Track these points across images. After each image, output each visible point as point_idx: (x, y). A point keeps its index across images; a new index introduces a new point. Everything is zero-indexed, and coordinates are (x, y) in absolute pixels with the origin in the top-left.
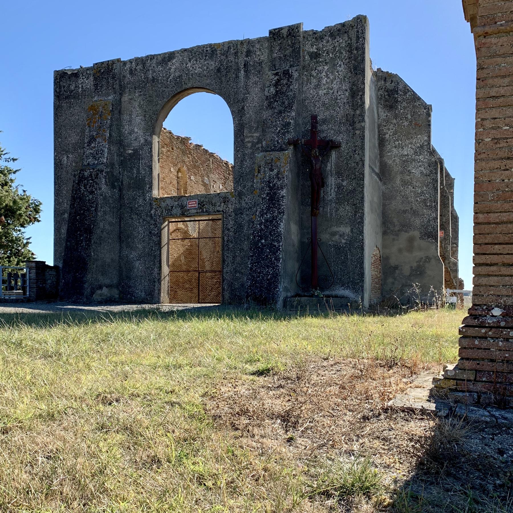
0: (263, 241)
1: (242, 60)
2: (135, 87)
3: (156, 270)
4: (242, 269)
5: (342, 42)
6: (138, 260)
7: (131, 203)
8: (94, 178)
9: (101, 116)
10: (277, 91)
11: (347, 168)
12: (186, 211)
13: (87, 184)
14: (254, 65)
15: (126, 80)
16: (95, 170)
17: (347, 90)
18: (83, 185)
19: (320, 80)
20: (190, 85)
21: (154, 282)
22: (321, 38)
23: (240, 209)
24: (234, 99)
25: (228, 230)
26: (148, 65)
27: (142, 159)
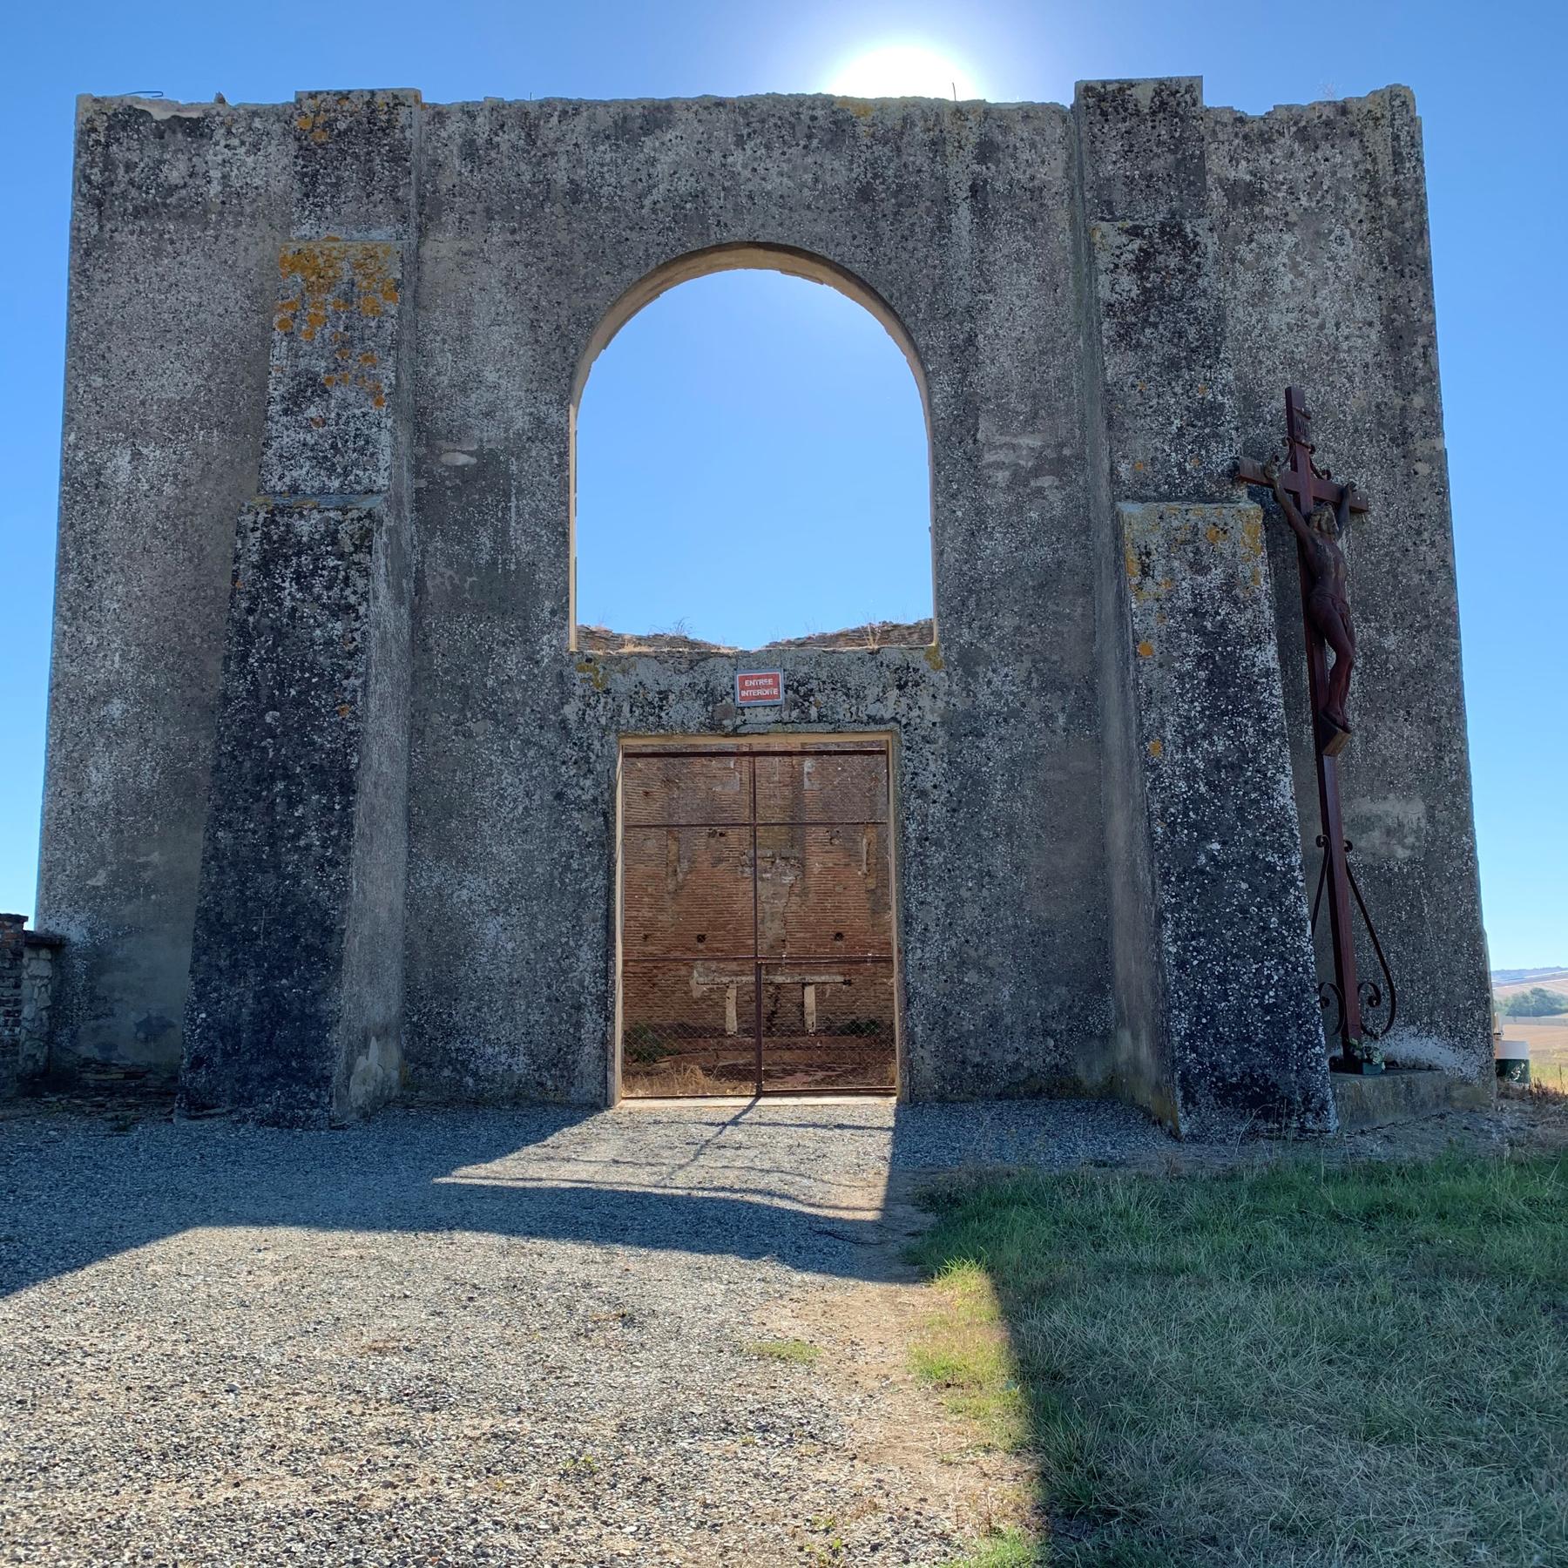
0: (1216, 846)
1: (960, 170)
2: (488, 210)
3: (586, 954)
4: (989, 953)
5: (1342, 165)
6: (495, 911)
7: (461, 669)
8: (348, 548)
9: (349, 302)
10: (1145, 291)
11: (1395, 587)
12: (727, 713)
13: (313, 573)
14: (1010, 195)
15: (446, 181)
16: (354, 514)
17: (1371, 324)
18: (289, 573)
19: (1268, 276)
20: (740, 233)
21: (579, 1008)
22: (1266, 139)
23: (969, 716)
24: (931, 304)
25: (923, 794)
26: (552, 136)
27: (520, 491)
